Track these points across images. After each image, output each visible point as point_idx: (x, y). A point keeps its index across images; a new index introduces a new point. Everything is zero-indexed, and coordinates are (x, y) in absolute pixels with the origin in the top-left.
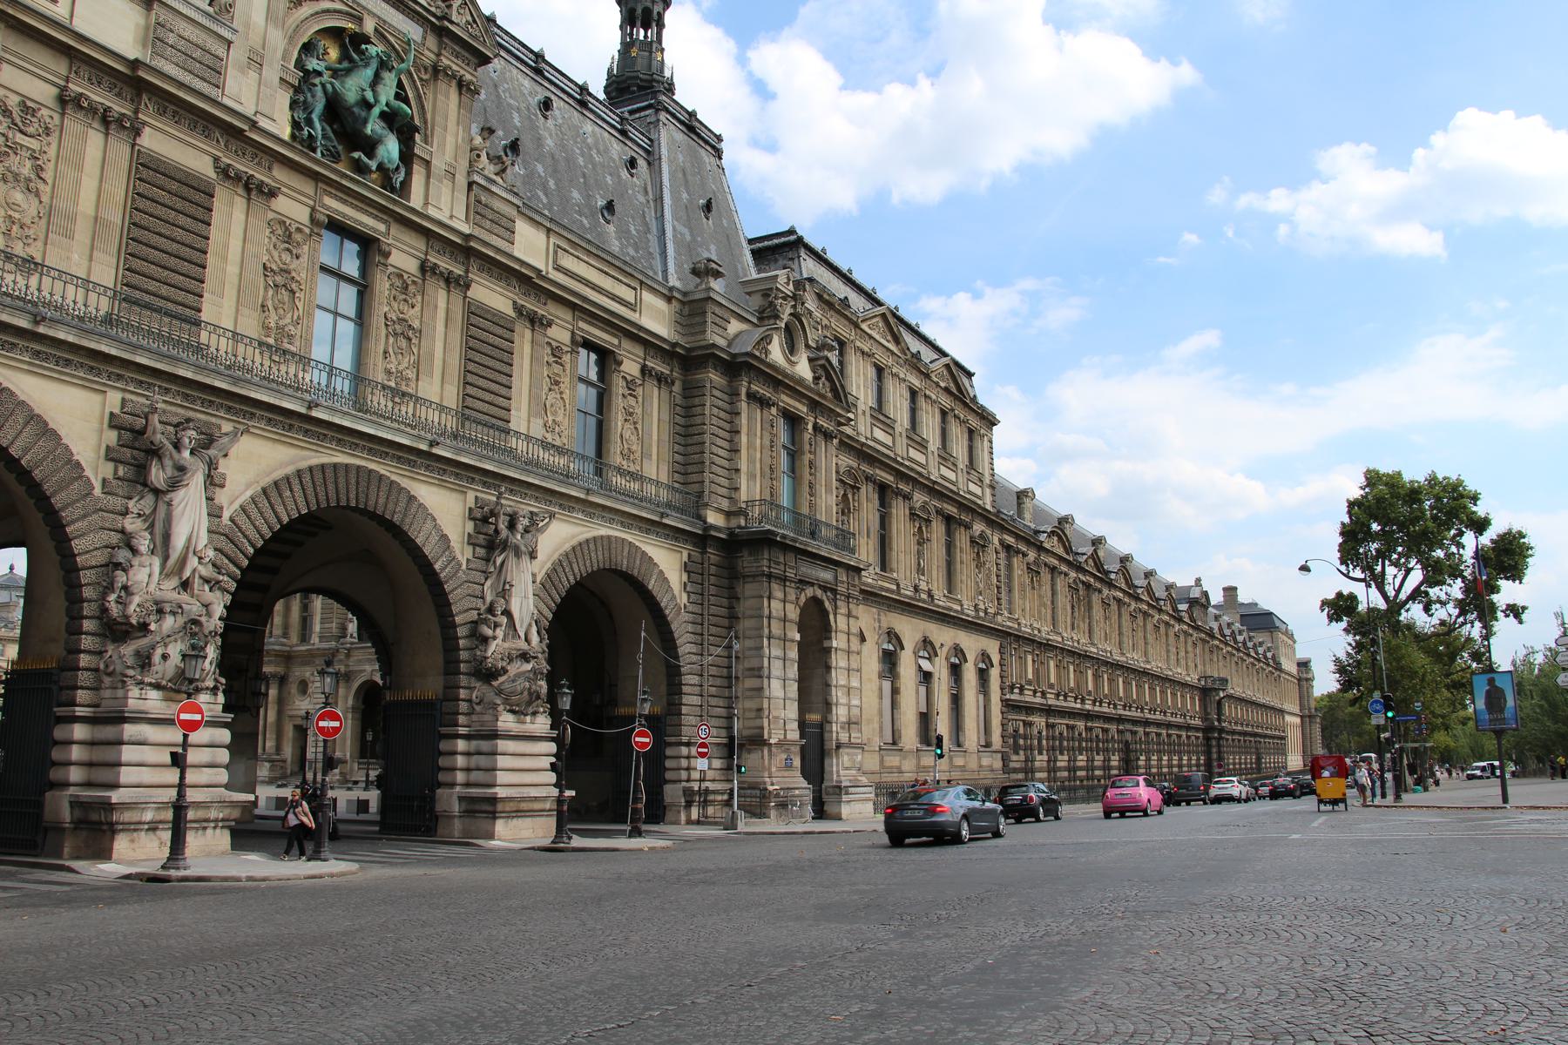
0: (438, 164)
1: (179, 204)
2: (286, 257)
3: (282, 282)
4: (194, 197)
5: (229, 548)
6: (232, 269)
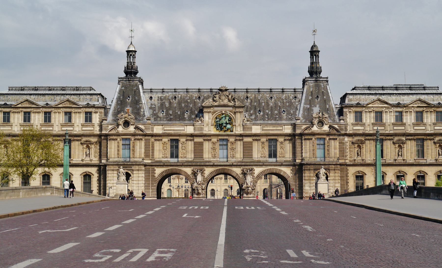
0: (237, 125)
3: (214, 149)
4: (201, 144)
6: (207, 150)
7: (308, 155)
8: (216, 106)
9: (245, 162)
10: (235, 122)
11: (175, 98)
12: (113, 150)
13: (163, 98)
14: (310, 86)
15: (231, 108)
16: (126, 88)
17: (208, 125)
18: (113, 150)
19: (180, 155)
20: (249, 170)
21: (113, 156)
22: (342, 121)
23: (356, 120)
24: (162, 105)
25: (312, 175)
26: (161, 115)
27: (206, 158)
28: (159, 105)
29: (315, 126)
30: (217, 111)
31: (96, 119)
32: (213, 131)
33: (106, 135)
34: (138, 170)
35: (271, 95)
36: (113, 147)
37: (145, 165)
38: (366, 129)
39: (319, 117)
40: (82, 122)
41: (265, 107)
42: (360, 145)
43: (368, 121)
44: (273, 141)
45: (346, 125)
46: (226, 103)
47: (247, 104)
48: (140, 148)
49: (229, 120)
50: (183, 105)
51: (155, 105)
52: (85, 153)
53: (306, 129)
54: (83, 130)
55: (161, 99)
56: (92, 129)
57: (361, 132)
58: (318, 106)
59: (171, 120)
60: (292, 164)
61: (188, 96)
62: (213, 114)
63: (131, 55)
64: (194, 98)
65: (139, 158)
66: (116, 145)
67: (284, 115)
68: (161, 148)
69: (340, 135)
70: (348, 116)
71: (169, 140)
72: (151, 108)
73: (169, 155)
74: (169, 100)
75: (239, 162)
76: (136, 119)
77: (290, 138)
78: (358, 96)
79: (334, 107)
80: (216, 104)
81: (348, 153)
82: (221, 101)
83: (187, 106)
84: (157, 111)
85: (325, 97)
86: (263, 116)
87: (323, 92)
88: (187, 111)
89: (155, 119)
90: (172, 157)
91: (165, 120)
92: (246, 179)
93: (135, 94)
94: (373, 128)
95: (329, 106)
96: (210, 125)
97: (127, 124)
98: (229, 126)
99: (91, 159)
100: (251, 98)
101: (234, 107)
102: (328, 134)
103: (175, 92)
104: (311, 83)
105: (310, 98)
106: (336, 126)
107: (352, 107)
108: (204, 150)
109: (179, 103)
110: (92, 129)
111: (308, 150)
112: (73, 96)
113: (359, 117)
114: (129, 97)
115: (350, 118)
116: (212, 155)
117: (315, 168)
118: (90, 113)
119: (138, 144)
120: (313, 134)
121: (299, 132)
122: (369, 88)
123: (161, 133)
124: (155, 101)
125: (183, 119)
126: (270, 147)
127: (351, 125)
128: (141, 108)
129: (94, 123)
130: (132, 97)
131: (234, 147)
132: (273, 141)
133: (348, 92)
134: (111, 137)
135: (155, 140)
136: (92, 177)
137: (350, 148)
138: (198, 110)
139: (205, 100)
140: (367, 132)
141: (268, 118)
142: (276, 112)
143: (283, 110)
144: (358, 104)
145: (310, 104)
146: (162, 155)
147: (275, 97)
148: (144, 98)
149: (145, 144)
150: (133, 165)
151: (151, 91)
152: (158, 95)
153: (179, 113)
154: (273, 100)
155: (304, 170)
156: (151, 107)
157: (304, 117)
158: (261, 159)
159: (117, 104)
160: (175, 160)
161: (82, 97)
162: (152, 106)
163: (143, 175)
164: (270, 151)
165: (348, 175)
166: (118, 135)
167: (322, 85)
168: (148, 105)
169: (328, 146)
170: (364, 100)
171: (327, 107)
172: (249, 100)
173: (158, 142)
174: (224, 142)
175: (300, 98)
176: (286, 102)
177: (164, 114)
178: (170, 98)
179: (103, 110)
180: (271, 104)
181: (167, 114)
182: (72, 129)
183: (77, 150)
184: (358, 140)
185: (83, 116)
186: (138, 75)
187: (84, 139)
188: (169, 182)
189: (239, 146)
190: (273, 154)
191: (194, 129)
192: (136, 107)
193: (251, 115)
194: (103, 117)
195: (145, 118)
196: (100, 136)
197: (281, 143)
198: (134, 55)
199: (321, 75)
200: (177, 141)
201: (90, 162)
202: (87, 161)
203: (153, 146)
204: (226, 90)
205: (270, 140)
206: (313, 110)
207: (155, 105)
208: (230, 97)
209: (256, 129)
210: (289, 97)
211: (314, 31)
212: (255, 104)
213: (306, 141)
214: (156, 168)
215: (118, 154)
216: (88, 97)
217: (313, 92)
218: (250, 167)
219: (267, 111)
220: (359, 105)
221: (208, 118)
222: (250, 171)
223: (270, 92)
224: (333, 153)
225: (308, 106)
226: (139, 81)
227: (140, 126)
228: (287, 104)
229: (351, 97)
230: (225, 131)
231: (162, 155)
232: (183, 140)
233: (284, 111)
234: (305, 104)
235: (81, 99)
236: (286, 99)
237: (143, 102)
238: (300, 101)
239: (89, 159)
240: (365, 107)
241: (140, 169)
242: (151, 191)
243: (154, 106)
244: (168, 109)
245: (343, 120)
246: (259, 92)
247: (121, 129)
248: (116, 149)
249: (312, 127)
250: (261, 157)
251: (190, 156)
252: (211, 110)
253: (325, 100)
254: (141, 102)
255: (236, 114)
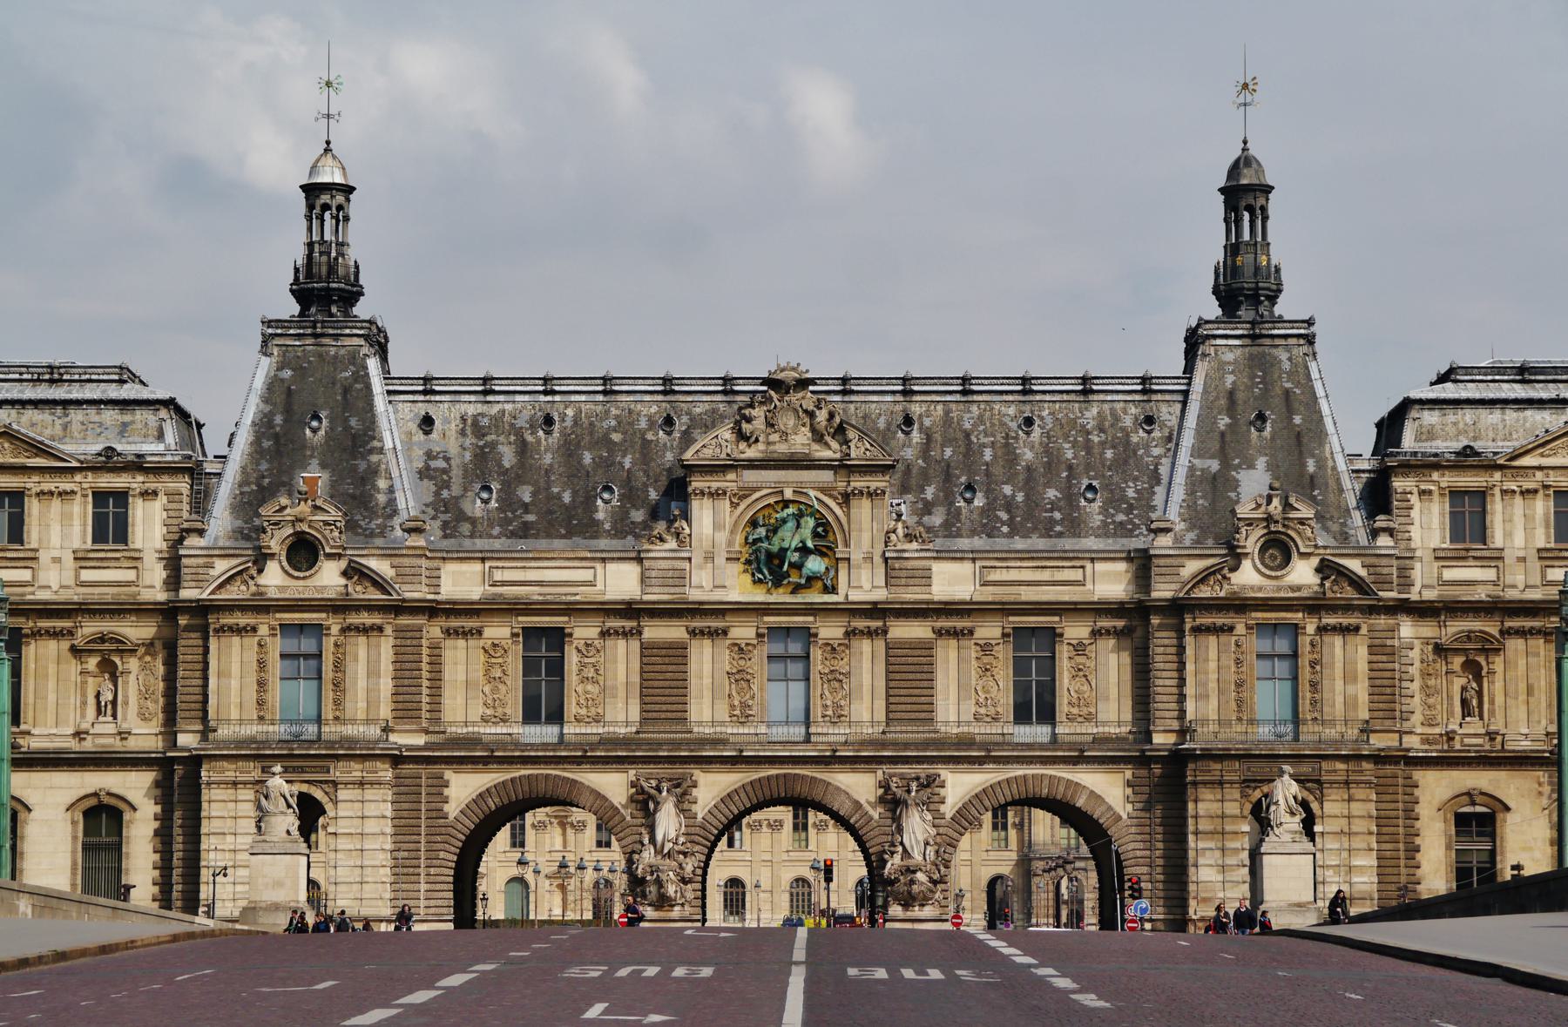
0: (856, 556)
1: (667, 660)
2: (742, 662)
3: (740, 677)
4: (677, 653)
5: (702, 832)
6: (707, 681)
7: (1211, 709)
8: (752, 465)
9: (895, 744)
10: (847, 544)
11: (549, 421)
12: (235, 683)
13: (485, 422)
14: (1222, 365)
15: (826, 476)
16: (300, 372)
17: (710, 557)
18: (235, 683)
19: (571, 708)
20: (914, 786)
21: (234, 715)
22: (1384, 541)
23: (1457, 534)
24: (483, 458)
25: (1232, 808)
26: (476, 508)
27: (700, 723)
28: (468, 456)
29: (1246, 565)
30: (755, 490)
31: (149, 525)
32: (739, 587)
33: (202, 610)
34: (361, 784)
35: (1028, 407)
36: (235, 668)
37: (397, 760)
38: (1509, 580)
39: (1269, 519)
40: (77, 544)
41: (997, 470)
42: (1474, 659)
43: (1519, 540)
44: (1034, 638)
45: (1405, 561)
46: (799, 449)
47: (909, 454)
48: (373, 673)
49: (815, 535)
50: (587, 458)
51: (447, 459)
52: (91, 701)
53: (1203, 578)
54: (83, 584)
55: (474, 427)
56: (130, 575)
57: (1481, 594)
58: (1261, 463)
59: (525, 531)
60: (1133, 754)
61: (614, 411)
62: (734, 505)
63: (326, 207)
64: (643, 424)
65: (368, 722)
66: (252, 656)
67: (1093, 511)
68: (478, 673)
69: (1372, 610)
70: (1415, 513)
71: (514, 635)
72: (424, 473)
73: (515, 708)
74: (519, 432)
75: (864, 743)
76: (351, 526)
77: (1120, 624)
78: (1468, 415)
79: (1342, 465)
80: (752, 453)
81: (1417, 699)
82: (775, 437)
83: (606, 464)
84: (456, 490)
85: (1297, 420)
86: (983, 511)
87: (1287, 392)
88: (607, 488)
89: (449, 530)
90: (531, 715)
91: (496, 531)
92: (900, 830)
93: (346, 405)
94: (1543, 576)
95: (1321, 464)
96: (720, 560)
97: (304, 552)
98: (815, 564)
99: (125, 726)
100: (927, 422)
101: (843, 467)
102: (1314, 606)
103: (545, 393)
104: (1228, 350)
105: (1224, 421)
106: (1355, 565)
107: (1436, 466)
108: (693, 682)
109: (569, 449)
110: (130, 575)
111: (1213, 685)
112: (31, 414)
113: (1469, 523)
114: (316, 417)
115: (1426, 522)
116: (733, 707)
117: (1249, 775)
118: (122, 497)
119: (362, 653)
120: (1239, 605)
121: (1169, 595)
122: (1524, 373)
123: (476, 596)
124: (449, 439)
125: (590, 529)
126: (1020, 667)
127: (1429, 557)
128: (374, 472)
129: (138, 545)
130: (332, 420)
131: (842, 666)
132: (1034, 638)
133: (1415, 394)
134: (227, 620)
135: (448, 633)
136: (127, 816)
137: (1426, 675)
138: (664, 481)
139: (696, 433)
140: (1512, 594)
141: (1011, 523)
142: (1052, 493)
143: (1085, 482)
144: (1468, 451)
145: (1223, 456)
146: (481, 710)
147: (1049, 420)
148: (393, 423)
149: (398, 651)
150: (337, 757)
151: (428, 386)
152: (463, 407)
153: (567, 497)
154: (1036, 432)
155: (1195, 784)
156: (428, 468)
157: (1192, 516)
158: (976, 729)
159: (256, 451)
160: (548, 733)
161: (76, 416)
162: (433, 464)
163: (388, 810)
164: (1021, 689)
165: (1418, 809)
166: (262, 606)
167: (1284, 356)
168: (410, 460)
169: (1313, 664)
170: (1497, 432)
171: (1311, 466)
172: (916, 436)
173: (461, 643)
174: (792, 643)
175: (1174, 422)
176: (1102, 443)
177: (494, 504)
178: (521, 422)
179: (183, 485)
180: (1029, 455)
181: (509, 501)
182: (26, 575)
183: (52, 685)
184: (1469, 635)
185: (81, 513)
186: (361, 310)
187: (89, 628)
188: (518, 841)
189: (867, 664)
190: (1035, 702)
191: (643, 579)
192: (354, 469)
193: (927, 508)
194: (185, 515)
195: (397, 521)
196: (168, 612)
197: (1079, 648)
198: (340, 208)
199: (1278, 310)
200: (558, 637)
201: (117, 744)
202: (103, 735)
203: (436, 664)
204: (803, 383)
205: (1019, 636)
206: (1235, 485)
207: (447, 459)
208: (821, 416)
209: (952, 581)
210: (1116, 419)
211: (1245, 86)
212: (948, 452)
213: (1202, 638)
214: (449, 775)
215: (260, 703)
216: (110, 416)
217: (1240, 396)
218: (921, 770)
219: (1007, 490)
220: (1471, 460)
221: (711, 522)
222: (922, 786)
223: (1024, 392)
224: (1339, 700)
225: (1214, 465)
226: (366, 337)
227: (373, 563)
228: (1109, 454)
229: (1430, 417)
230: (797, 589)
231: (481, 710)
232: (584, 631)
233: (1090, 487)
234: (1197, 452)
235: (75, 428)
236: (1102, 430)
237: (388, 444)
238: (1172, 439)
239: (111, 729)
240: (1501, 467)
241: (370, 777)
242: (423, 887)
243: (440, 464)
244: (511, 481)
245: (1390, 532)
246: (964, 393)
247: (274, 578)
248: (252, 680)
249: (1234, 569)
250: (977, 718)
251: (624, 717)
252: (729, 481)
253: (1298, 435)
254: (376, 444)
255: (854, 502)
